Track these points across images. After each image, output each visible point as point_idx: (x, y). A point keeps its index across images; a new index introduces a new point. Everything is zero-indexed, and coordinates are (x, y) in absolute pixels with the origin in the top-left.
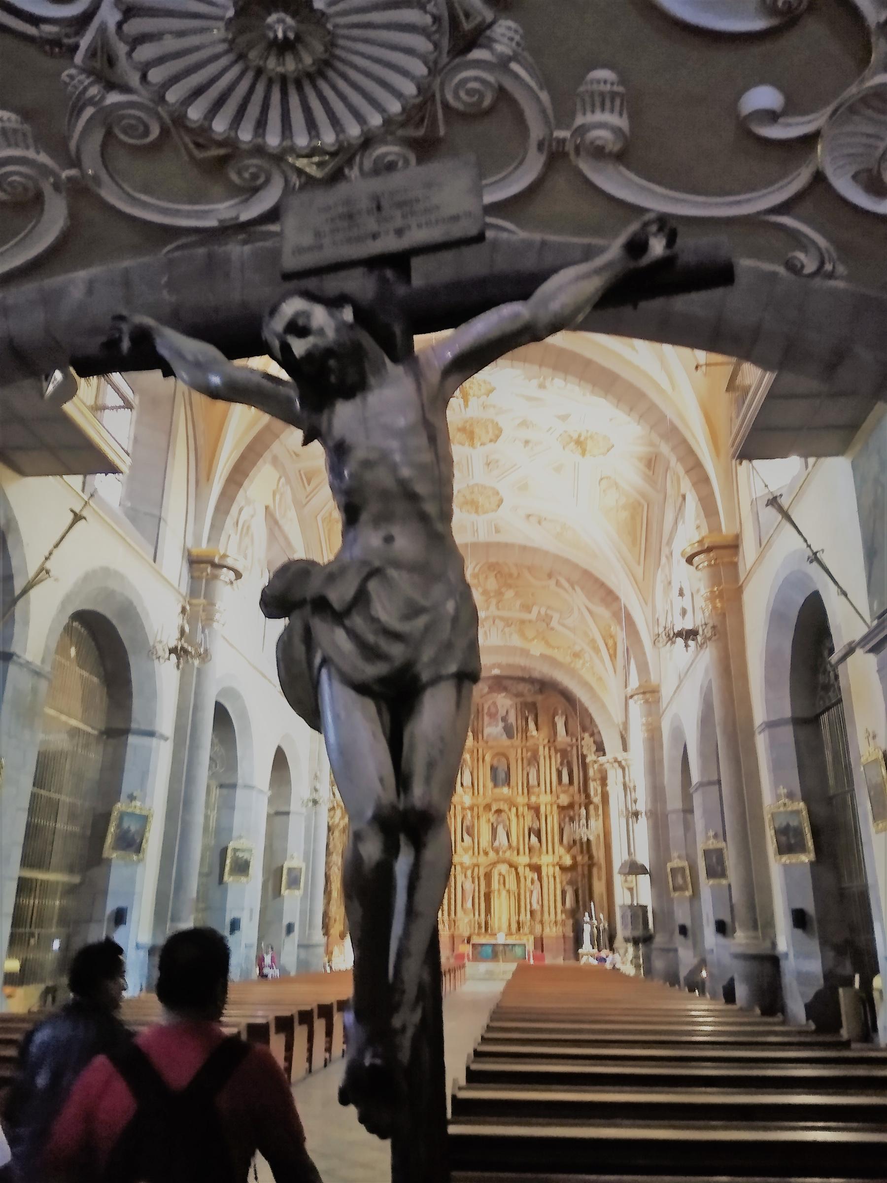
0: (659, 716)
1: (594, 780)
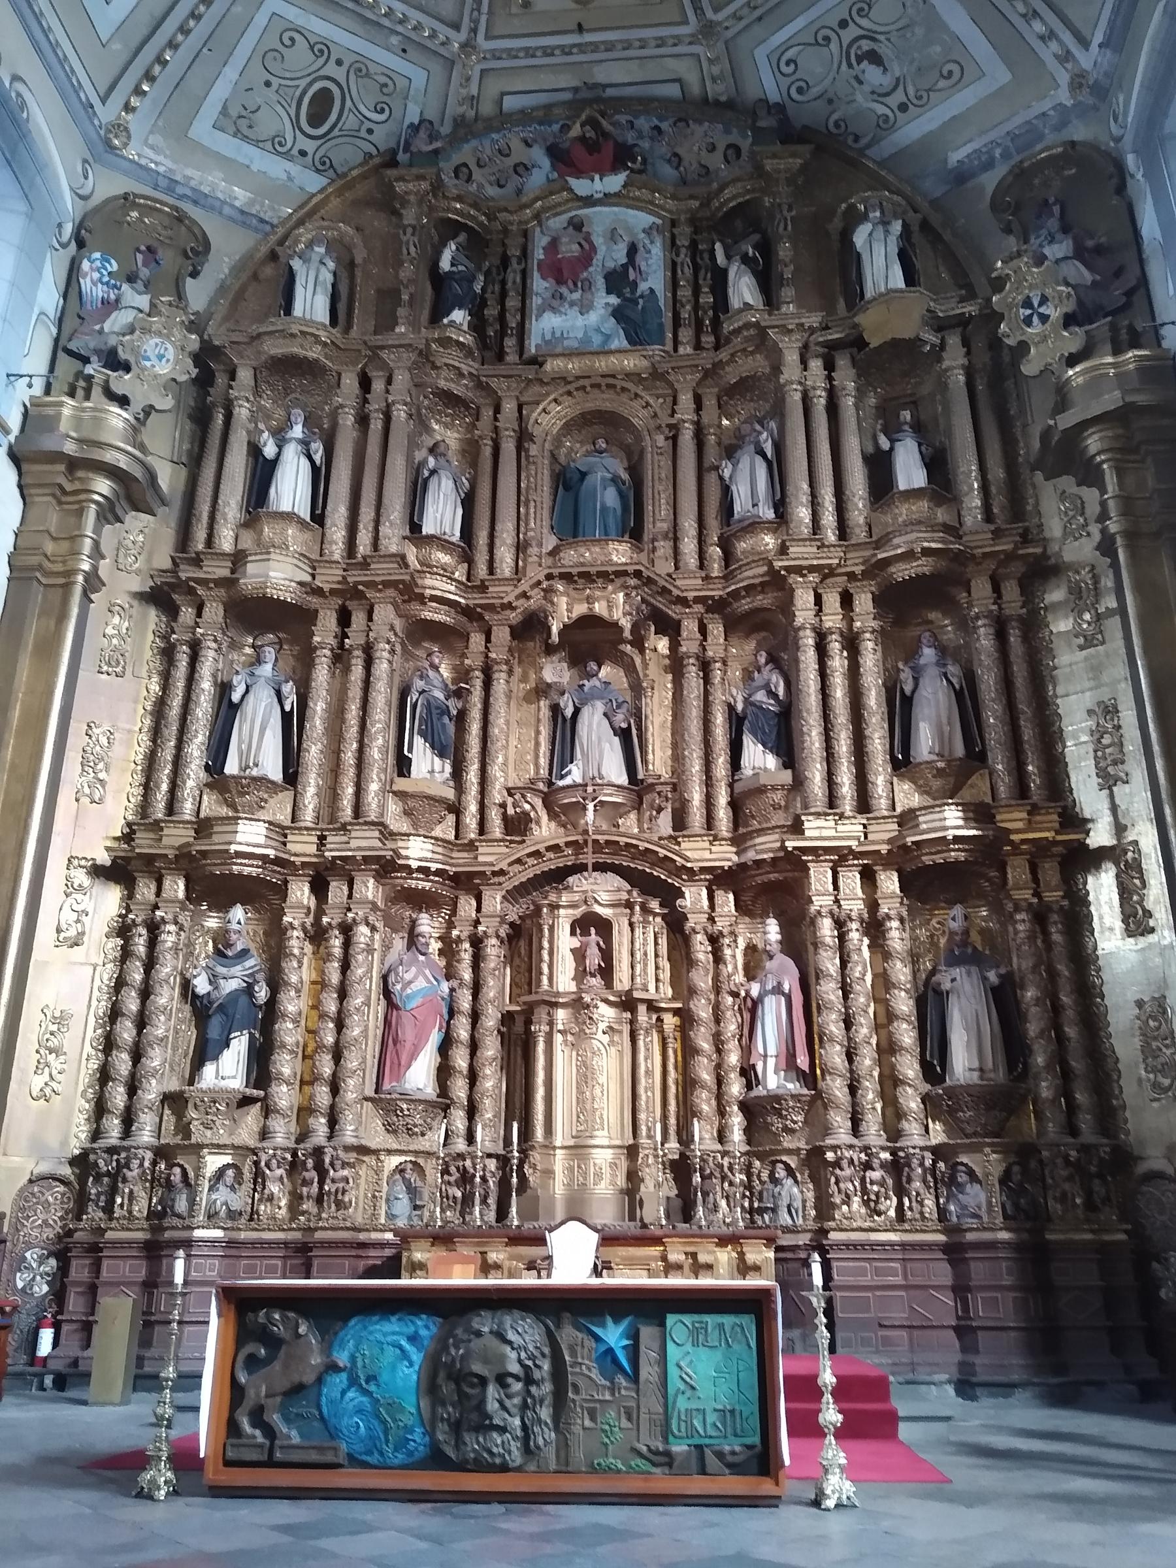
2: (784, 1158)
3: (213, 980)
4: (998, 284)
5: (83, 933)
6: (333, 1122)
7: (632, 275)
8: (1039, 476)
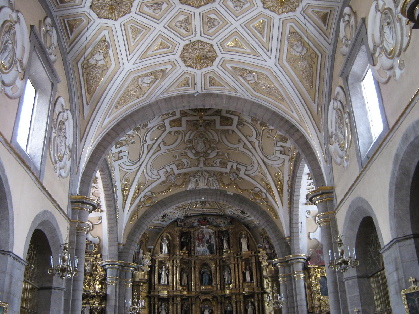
0: (334, 212)
1: (267, 278)
4: (259, 252)
7: (210, 241)
8: (264, 279)
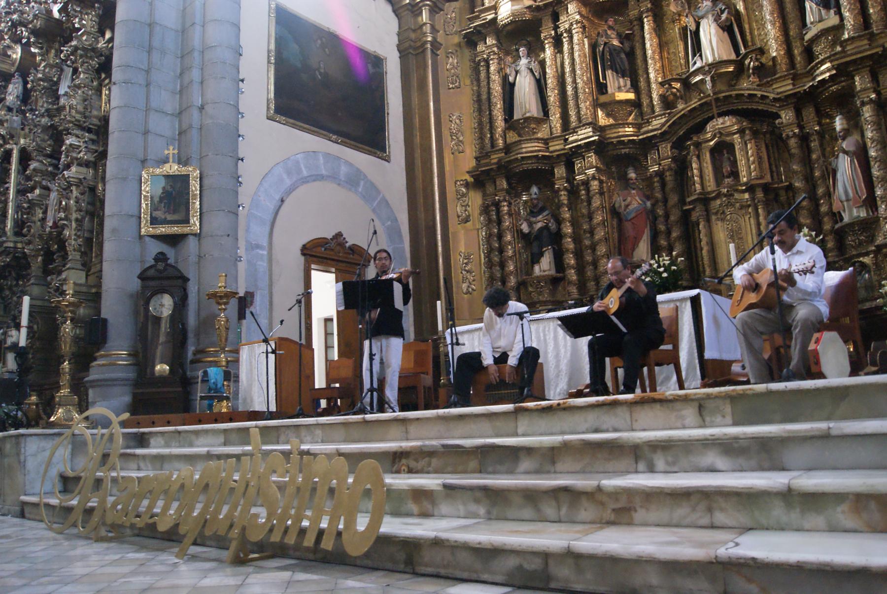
2: (861, 259)
3: (530, 225)
5: (469, 216)
6: (598, 283)
